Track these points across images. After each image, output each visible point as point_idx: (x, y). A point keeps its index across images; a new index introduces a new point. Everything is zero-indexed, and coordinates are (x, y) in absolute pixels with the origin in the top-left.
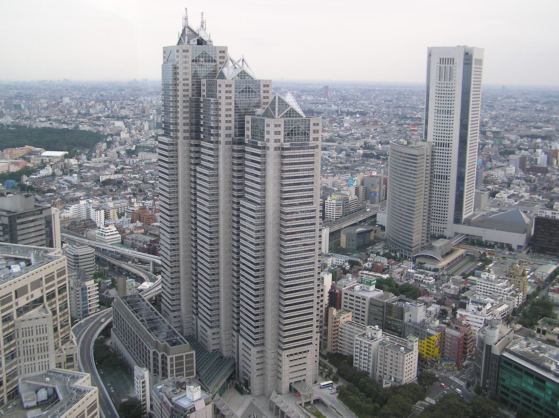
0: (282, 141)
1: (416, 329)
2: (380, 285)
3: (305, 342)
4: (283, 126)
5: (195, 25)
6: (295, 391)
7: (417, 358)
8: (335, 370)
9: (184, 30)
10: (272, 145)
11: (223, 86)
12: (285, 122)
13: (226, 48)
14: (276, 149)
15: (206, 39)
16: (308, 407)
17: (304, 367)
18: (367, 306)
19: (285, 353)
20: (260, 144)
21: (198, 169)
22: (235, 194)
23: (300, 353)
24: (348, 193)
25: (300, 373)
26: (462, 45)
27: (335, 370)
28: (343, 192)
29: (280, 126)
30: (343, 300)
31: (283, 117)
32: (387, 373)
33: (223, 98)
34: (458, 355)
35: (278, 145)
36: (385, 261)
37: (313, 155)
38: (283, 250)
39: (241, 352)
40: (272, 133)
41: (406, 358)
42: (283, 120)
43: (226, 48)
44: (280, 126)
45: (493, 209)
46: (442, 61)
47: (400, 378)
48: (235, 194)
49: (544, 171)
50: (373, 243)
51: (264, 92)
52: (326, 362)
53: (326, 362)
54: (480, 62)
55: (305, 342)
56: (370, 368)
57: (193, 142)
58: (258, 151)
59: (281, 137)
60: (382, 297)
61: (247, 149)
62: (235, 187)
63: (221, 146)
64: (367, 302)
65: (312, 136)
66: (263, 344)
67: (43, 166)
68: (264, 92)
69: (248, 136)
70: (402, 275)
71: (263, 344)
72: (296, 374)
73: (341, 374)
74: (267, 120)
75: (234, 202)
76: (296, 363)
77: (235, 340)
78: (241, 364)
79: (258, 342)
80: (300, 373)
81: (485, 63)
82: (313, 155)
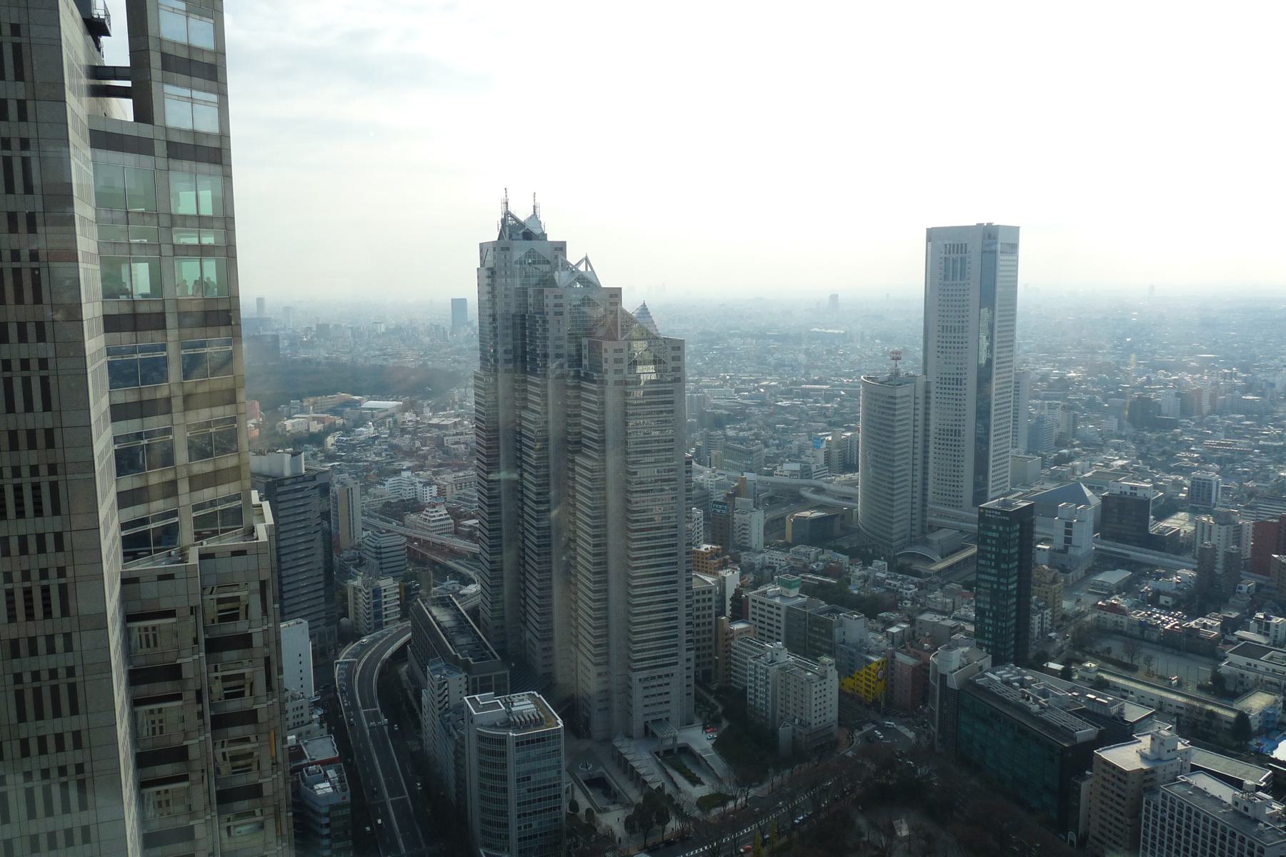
0: (626, 371)
1: (851, 653)
2: (806, 589)
3: (667, 661)
5: (523, 214)
6: (654, 735)
7: (836, 694)
9: (504, 221)
10: (611, 377)
11: (551, 296)
13: (564, 243)
14: (617, 383)
15: (537, 231)
17: (666, 698)
18: (782, 619)
19: (636, 676)
21: (524, 414)
24: (812, 460)
25: (661, 708)
26: (985, 221)
27: (720, 710)
28: (804, 458)
30: (751, 610)
32: (791, 712)
33: (551, 313)
35: (618, 377)
36: (844, 559)
43: (564, 243)
52: (712, 700)
54: (1013, 247)
55: (667, 661)
56: (769, 705)
57: (517, 377)
63: (550, 382)
64: (782, 612)
67: (361, 421)
70: (866, 581)
72: (652, 709)
76: (654, 691)
80: (661, 708)
82: (671, 392)
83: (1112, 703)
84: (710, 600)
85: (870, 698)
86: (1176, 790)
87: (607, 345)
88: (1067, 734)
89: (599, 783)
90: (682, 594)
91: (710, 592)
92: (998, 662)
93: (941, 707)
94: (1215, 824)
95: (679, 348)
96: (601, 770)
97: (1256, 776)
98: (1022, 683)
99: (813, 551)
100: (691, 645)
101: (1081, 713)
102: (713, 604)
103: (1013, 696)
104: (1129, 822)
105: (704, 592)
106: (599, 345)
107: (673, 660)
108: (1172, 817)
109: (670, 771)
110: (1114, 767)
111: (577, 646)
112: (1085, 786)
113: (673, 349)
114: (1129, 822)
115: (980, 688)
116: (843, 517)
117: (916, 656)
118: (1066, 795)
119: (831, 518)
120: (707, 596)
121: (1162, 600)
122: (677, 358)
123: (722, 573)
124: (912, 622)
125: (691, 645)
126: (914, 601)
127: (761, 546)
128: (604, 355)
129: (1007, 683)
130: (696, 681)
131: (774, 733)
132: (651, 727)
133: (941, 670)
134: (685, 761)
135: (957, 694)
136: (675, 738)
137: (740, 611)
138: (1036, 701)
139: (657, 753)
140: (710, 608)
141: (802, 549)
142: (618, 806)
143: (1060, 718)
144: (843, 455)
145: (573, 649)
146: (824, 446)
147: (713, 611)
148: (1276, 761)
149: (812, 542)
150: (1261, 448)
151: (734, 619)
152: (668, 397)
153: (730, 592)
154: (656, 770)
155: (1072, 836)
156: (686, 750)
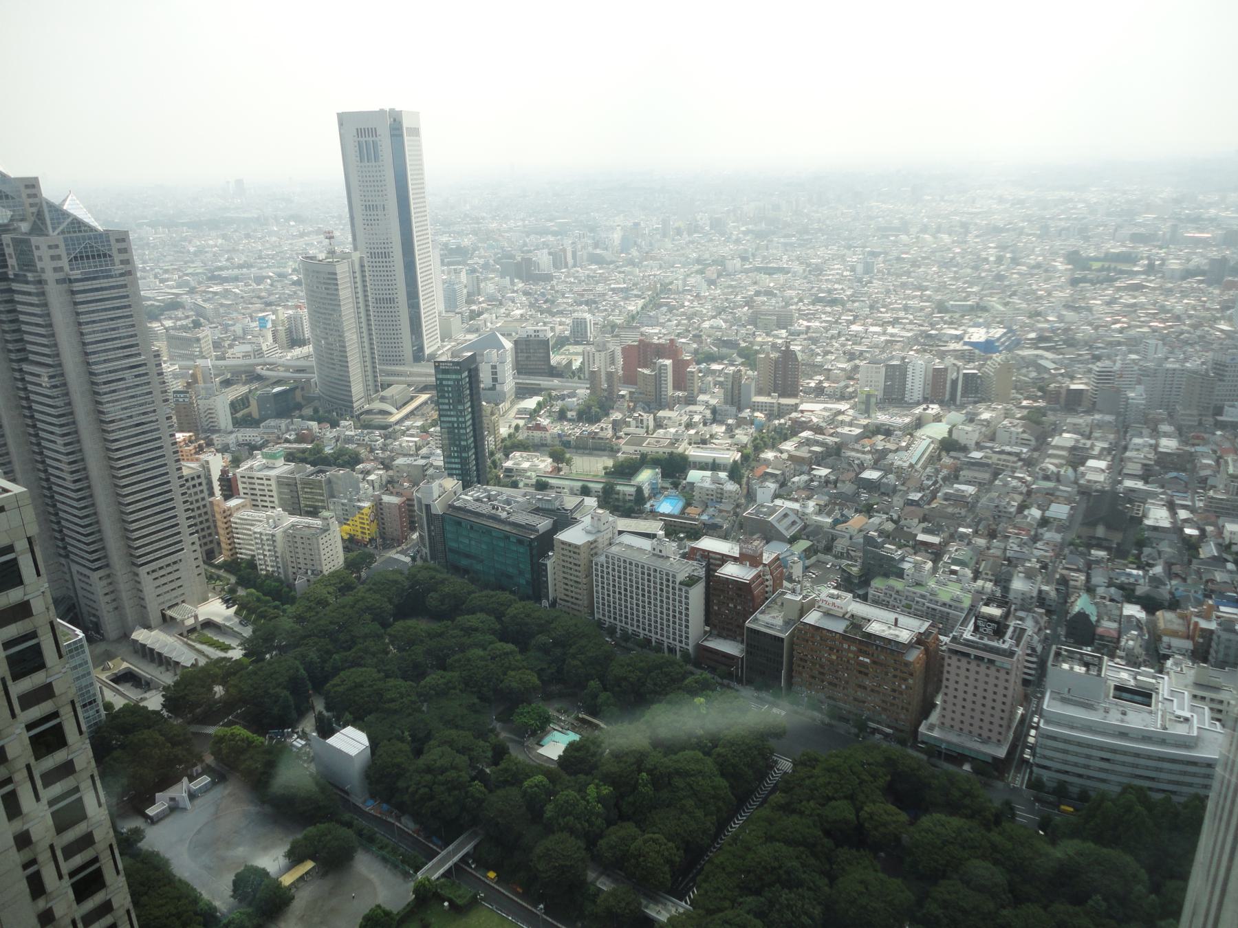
0: (67, 268)
2: (290, 457)
3: (172, 549)
4: (62, 246)
6: (172, 618)
8: (233, 580)
10: (50, 276)
12: (65, 240)
14: (58, 281)
16: (193, 636)
18: (274, 487)
19: (143, 571)
20: (30, 276)
22: (13, 356)
23: (168, 565)
26: (387, 108)
27: (233, 580)
29: (57, 246)
30: (240, 486)
31: (63, 232)
32: (302, 566)
34: (402, 527)
35: (60, 275)
36: (314, 425)
37: (125, 286)
38: (106, 427)
39: (78, 585)
40: (47, 259)
41: (321, 542)
42: (61, 237)
44: (57, 246)
45: (469, 337)
46: (360, 132)
47: (319, 568)
48: (13, 356)
49: (548, 278)
50: (299, 407)
51: (29, 196)
53: (221, 572)
54: (415, 132)
55: (172, 549)
58: (30, 288)
59: (64, 263)
60: (292, 473)
61: (15, 286)
62: (10, 346)
64: (273, 482)
65: (117, 258)
66: (107, 565)
68: (29, 196)
69: (13, 266)
71: (107, 565)
73: (244, 582)
74: (35, 240)
75: (14, 370)
77: (66, 569)
78: (83, 601)
79: (97, 564)
81: (423, 132)
82: (125, 286)
83: (556, 498)
84: (200, 484)
85: (367, 537)
86: (614, 549)
87: (35, 240)
88: (531, 528)
89: (127, 678)
90: (175, 484)
91: (199, 477)
92: (466, 485)
93: (429, 531)
94: (643, 567)
95: (123, 240)
96: (125, 665)
97: (656, 527)
98: (489, 498)
99: (283, 423)
100: (193, 529)
101: (537, 511)
102: (204, 487)
103: (485, 509)
104: (585, 581)
105: (193, 479)
106: (27, 242)
107: (178, 547)
108: (614, 570)
109: (199, 646)
110: (570, 545)
111: (67, 556)
112: (549, 563)
113: (118, 241)
114: (585, 581)
115: (459, 509)
116: (303, 389)
117: (398, 494)
118: (539, 572)
119: (293, 390)
120: (196, 482)
121: (569, 414)
122: (124, 251)
123: (203, 457)
124: (387, 467)
125: (193, 529)
126: (383, 449)
127: (230, 427)
128: (36, 253)
129: (478, 500)
130: (205, 562)
131: (291, 587)
132: (169, 613)
133: (424, 502)
134: (210, 634)
135: (442, 518)
136: (196, 617)
137: (229, 488)
138: (503, 509)
139: (181, 635)
140: (202, 491)
141: (272, 422)
142: (154, 692)
143: (523, 518)
144: (289, 331)
145: (63, 561)
146: (269, 325)
147: (206, 493)
148: (663, 515)
149: (281, 414)
150: (613, 290)
151: (227, 497)
152: (122, 292)
153: (216, 475)
154: (185, 649)
155: (545, 603)
156: (209, 624)
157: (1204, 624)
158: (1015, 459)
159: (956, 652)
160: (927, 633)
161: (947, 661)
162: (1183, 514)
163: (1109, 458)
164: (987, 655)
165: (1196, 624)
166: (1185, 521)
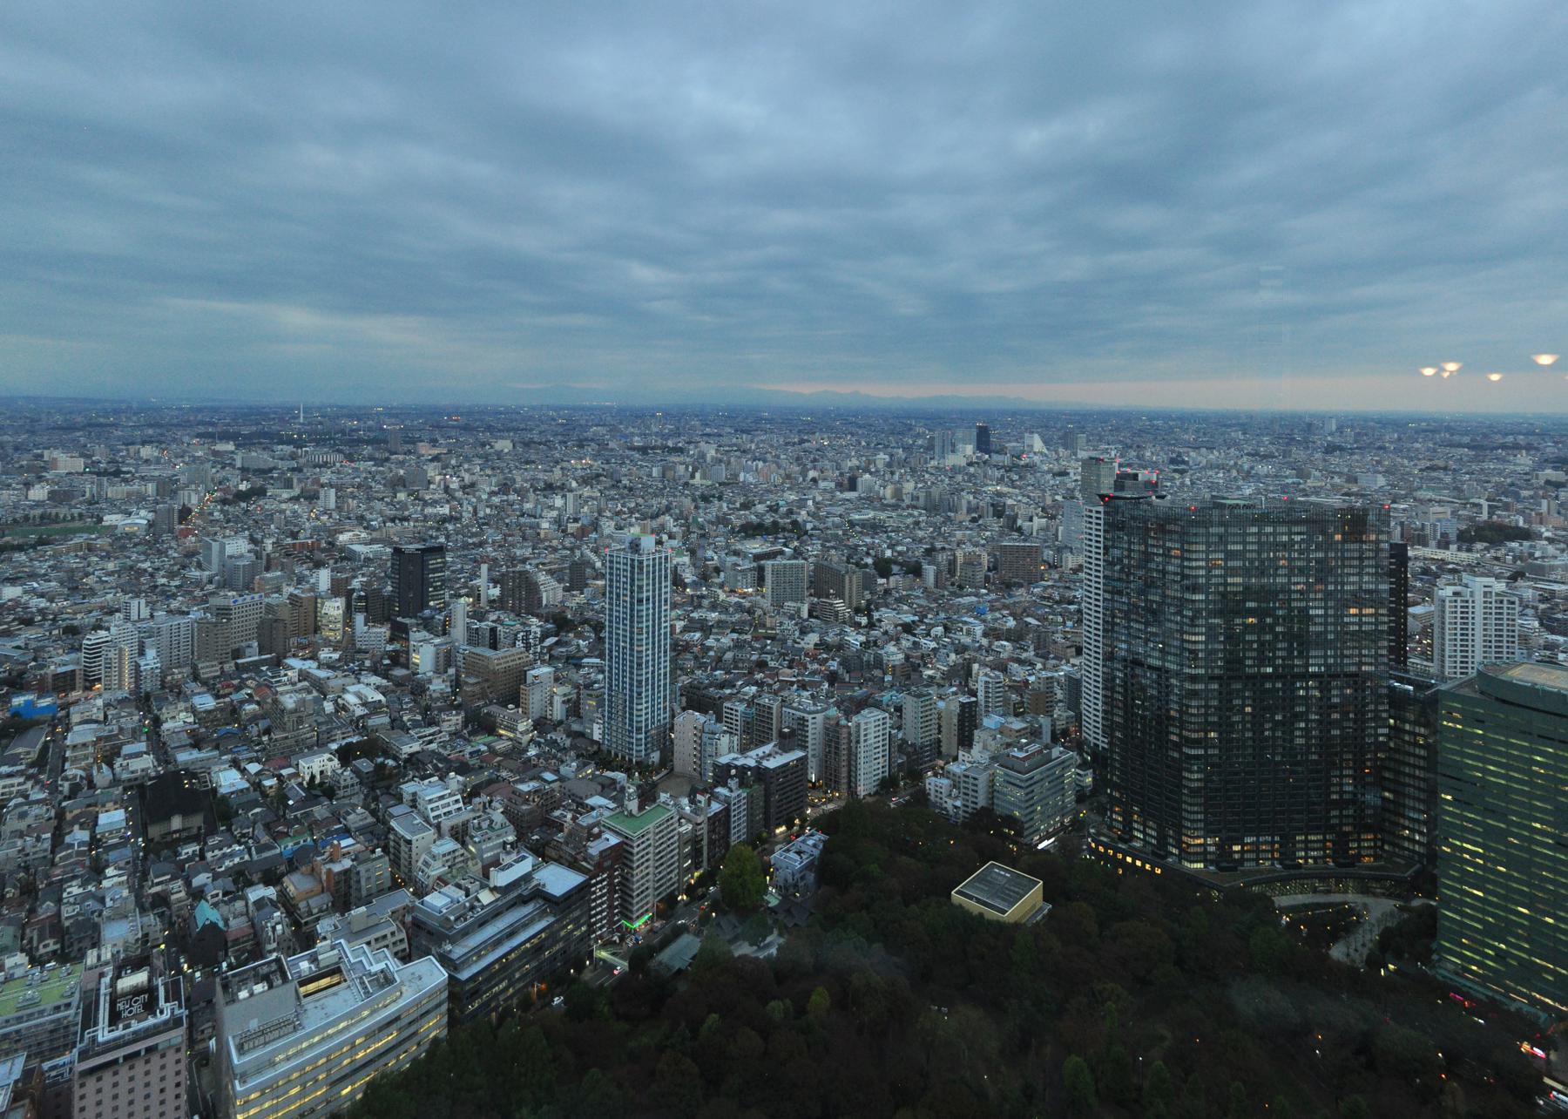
157: (337, 868)
158: (22, 780)
159: (92, 1071)
160: (27, 1074)
161: (77, 1092)
162: (253, 768)
163: (144, 738)
164: (141, 1046)
165: (329, 870)
166: (258, 774)
